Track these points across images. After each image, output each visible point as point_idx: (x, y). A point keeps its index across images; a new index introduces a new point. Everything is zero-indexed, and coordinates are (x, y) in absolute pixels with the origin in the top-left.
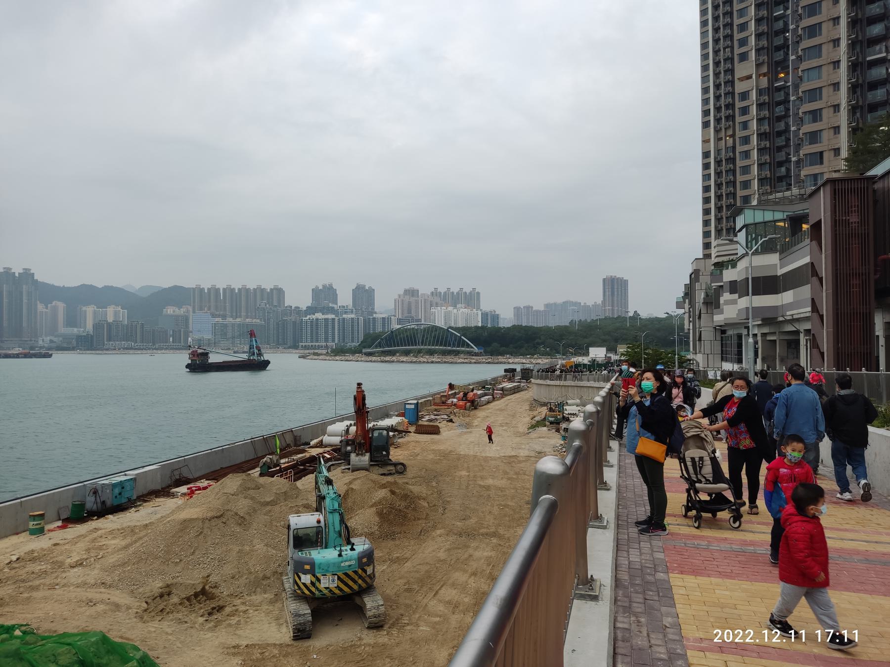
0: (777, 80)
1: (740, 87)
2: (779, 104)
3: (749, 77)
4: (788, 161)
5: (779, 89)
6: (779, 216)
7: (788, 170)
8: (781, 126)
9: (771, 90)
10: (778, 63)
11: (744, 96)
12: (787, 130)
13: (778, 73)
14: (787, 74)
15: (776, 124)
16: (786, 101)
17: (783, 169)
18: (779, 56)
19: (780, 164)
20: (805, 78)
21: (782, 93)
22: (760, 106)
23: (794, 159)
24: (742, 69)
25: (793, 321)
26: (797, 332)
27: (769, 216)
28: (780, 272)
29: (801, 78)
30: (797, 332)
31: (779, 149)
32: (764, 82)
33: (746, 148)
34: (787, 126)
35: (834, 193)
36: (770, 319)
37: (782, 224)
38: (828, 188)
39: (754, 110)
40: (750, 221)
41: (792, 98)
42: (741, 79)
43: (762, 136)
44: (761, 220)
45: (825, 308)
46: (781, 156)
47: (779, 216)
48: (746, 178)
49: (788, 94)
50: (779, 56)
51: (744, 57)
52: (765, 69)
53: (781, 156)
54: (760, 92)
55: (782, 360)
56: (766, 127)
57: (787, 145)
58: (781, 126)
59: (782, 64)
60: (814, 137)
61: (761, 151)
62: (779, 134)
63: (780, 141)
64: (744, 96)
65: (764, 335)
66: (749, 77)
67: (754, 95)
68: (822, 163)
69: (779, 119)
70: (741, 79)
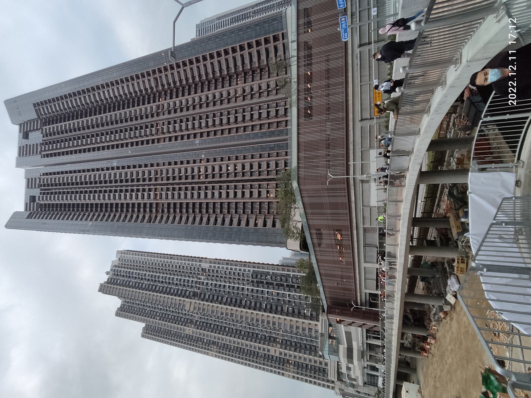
0: (279, 342)
1: (277, 354)
2: (286, 343)
3: (275, 350)
4: (305, 344)
5: (282, 342)
6: (327, 342)
7: (308, 345)
8: (293, 344)
9: (282, 344)
10: (274, 340)
11: (281, 353)
12: (295, 342)
13: (277, 341)
14: (278, 338)
15: (313, 316)
16: (286, 340)
17: (308, 346)
18: (272, 339)
19: (306, 347)
20: (286, 328)
21: (283, 341)
22: (285, 349)
23: (305, 342)
24: (272, 353)
25: (363, 343)
26: (367, 343)
27: (327, 346)
28: (346, 346)
29: (286, 330)
30: (367, 343)
31: (301, 346)
32: (279, 346)
33: (298, 357)
34: (294, 342)
35: (330, 314)
36: (362, 355)
37: (330, 342)
38: (328, 315)
39: (286, 351)
40: (327, 352)
41: (286, 338)
42: (275, 353)
43: (295, 350)
44: (328, 349)
45: (361, 322)
46: (303, 346)
47: (327, 342)
48: (308, 360)
49: (284, 339)
50: (272, 339)
51: (268, 351)
52: (275, 345)
53: (303, 346)
54: (281, 348)
55: (377, 353)
56: (293, 349)
57: (300, 343)
58: (293, 344)
59: (275, 339)
60: (304, 329)
61: (300, 352)
62: (296, 345)
63: (298, 345)
64: (281, 353)
65: (367, 360)
66: (275, 350)
67: (281, 350)
68: (312, 329)
69: (291, 344)
70: (275, 353)
